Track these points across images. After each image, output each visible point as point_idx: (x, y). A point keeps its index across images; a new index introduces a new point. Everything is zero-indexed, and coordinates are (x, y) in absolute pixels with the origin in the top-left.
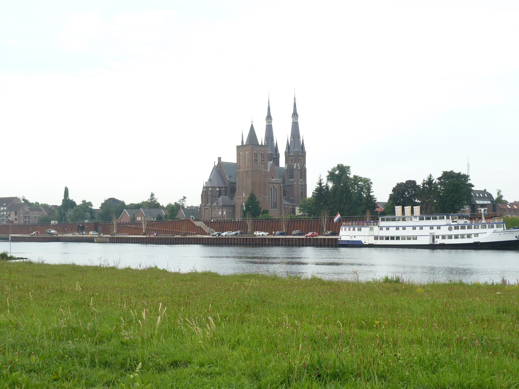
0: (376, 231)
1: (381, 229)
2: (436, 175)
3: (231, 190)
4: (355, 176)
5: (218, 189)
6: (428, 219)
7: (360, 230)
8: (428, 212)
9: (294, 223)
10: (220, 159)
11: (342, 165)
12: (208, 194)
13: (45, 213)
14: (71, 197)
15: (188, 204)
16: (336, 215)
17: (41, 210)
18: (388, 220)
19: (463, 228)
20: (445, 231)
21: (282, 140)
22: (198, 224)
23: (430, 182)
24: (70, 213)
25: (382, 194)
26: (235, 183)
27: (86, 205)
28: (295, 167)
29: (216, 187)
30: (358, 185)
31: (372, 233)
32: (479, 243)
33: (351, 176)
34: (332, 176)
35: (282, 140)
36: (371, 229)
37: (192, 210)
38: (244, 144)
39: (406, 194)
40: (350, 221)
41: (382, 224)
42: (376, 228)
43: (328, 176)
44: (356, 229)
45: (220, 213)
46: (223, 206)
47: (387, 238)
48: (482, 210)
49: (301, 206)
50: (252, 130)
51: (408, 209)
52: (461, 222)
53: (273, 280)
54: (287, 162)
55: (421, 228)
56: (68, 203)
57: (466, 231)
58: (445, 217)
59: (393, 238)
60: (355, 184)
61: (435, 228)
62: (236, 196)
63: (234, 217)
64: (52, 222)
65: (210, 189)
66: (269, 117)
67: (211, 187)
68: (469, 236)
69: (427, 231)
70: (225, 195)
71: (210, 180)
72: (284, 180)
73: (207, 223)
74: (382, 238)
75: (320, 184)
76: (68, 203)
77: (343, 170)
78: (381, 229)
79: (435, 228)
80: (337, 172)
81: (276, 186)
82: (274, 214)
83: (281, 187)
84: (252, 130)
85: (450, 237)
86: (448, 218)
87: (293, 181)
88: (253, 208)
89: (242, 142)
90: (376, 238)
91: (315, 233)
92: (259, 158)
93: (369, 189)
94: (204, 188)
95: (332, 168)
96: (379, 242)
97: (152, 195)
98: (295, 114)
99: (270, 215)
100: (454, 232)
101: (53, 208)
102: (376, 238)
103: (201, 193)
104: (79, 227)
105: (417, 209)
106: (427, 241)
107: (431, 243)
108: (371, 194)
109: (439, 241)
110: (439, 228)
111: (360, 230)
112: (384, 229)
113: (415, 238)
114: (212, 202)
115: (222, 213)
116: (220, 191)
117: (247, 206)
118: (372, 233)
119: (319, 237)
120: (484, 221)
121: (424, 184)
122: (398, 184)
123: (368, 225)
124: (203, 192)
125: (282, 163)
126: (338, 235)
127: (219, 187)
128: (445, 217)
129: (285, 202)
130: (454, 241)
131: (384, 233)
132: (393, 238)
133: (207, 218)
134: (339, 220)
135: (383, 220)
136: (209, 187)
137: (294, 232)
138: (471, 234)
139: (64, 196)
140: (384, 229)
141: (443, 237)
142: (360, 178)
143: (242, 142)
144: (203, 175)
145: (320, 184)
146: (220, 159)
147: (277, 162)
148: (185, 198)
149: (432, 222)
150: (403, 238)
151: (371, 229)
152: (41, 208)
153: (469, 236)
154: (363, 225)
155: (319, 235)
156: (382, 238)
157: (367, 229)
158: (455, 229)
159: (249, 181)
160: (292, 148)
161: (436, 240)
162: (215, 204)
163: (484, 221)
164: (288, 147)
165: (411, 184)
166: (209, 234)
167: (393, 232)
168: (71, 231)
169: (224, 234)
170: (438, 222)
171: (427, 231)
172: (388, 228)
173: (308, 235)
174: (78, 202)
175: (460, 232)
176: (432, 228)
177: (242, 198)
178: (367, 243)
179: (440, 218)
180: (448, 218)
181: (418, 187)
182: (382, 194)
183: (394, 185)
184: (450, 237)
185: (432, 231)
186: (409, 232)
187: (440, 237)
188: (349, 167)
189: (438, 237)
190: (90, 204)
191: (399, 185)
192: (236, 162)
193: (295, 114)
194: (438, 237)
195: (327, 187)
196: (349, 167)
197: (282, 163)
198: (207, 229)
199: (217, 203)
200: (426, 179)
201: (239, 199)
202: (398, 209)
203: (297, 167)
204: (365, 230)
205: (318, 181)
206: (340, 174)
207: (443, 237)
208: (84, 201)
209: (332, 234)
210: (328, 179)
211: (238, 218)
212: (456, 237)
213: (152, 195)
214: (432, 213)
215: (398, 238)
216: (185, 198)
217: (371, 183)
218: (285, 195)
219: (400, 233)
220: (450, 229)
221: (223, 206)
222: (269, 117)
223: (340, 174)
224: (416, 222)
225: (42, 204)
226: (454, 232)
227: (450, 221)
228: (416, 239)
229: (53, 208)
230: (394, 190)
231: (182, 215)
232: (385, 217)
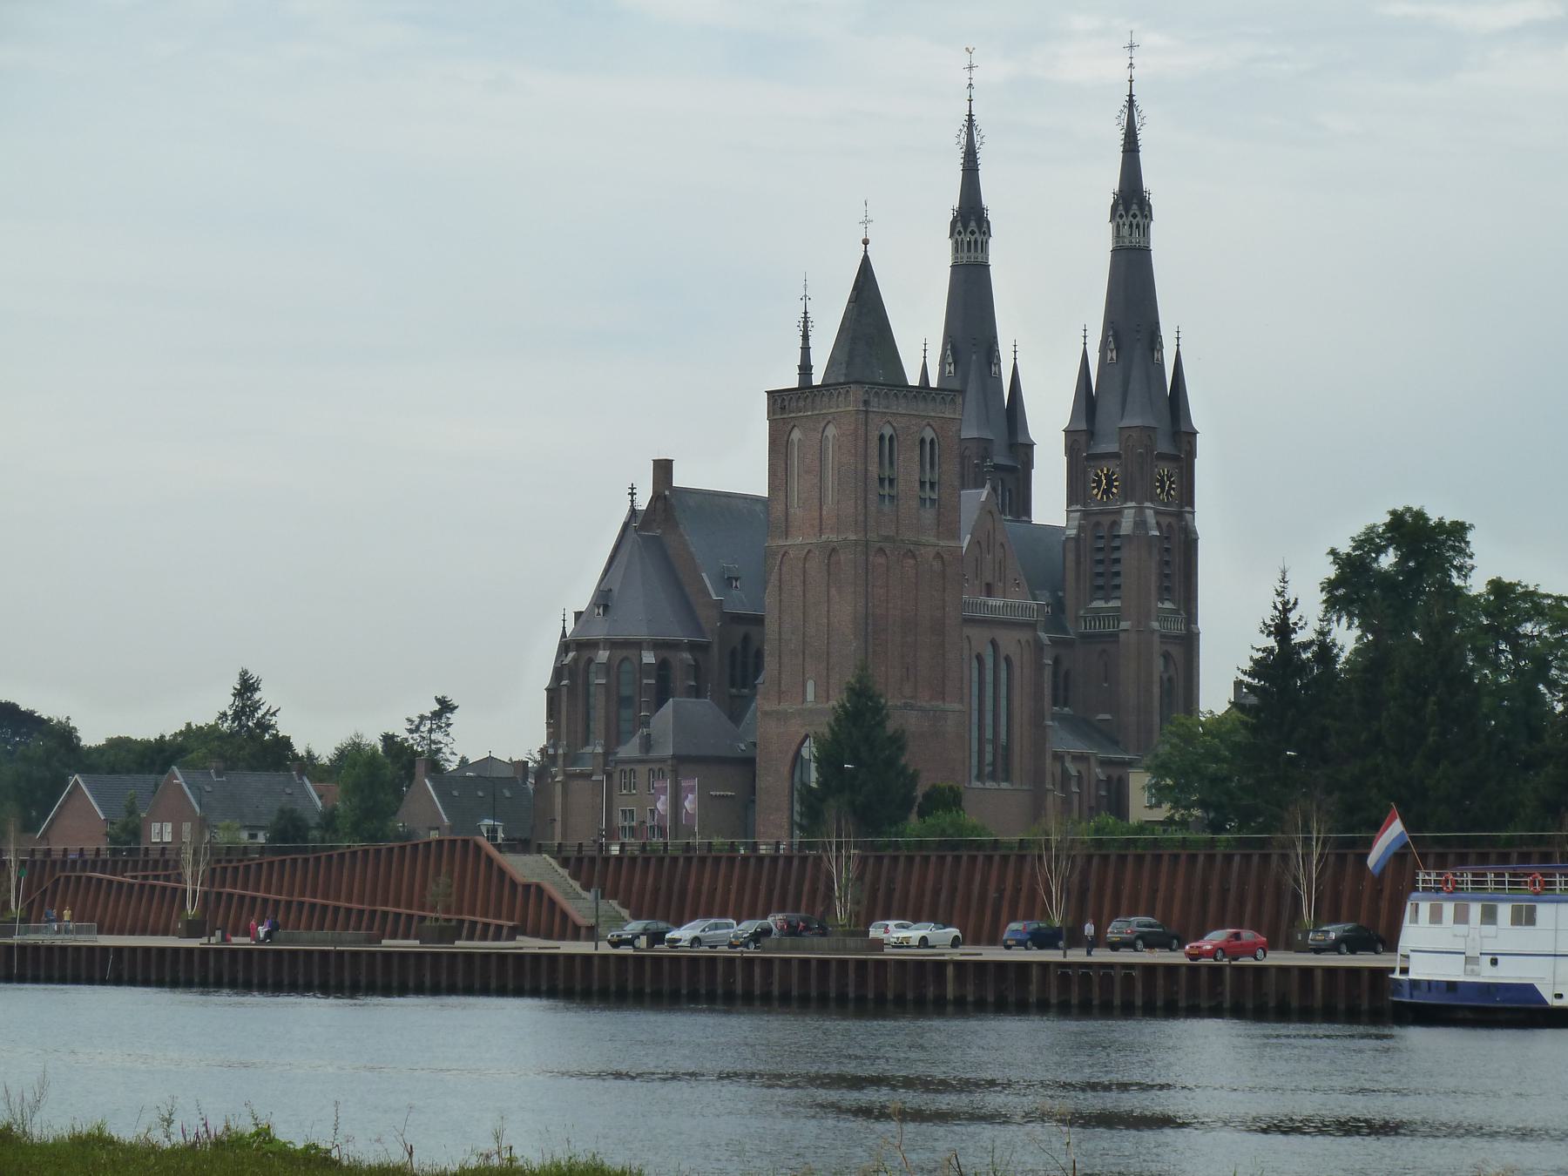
3: (730, 660)
4: (1498, 587)
5: (649, 658)
7: (1525, 917)
9: (1113, 873)
10: (663, 469)
11: (1420, 516)
12: (585, 681)
15: (465, 744)
16: (1377, 826)
21: (1048, 355)
22: (525, 867)
26: (759, 621)
28: (1126, 526)
29: (638, 645)
30: (1514, 639)
33: (1477, 585)
34: (1352, 584)
35: (1048, 355)
37: (488, 783)
38: (817, 379)
40: (1462, 860)
43: (1330, 586)
44: (1504, 911)
45: (663, 805)
49: (1161, 769)
50: (865, 291)
54: (1076, 491)
60: (1495, 632)
62: (763, 703)
63: (745, 826)
65: (603, 655)
66: (970, 220)
67: (613, 645)
70: (697, 692)
71: (604, 599)
72: (1058, 606)
73: (582, 865)
75: (1282, 630)
80: (1387, 560)
81: (1010, 642)
82: (995, 812)
83: (1038, 647)
84: (865, 291)
87: (1117, 614)
88: (865, 772)
89: (805, 368)
91: (1247, 935)
92: (908, 469)
94: (565, 646)
95: (1358, 529)
97: (247, 687)
98: (1131, 203)
99: (970, 817)
103: (546, 678)
111: (1525, 917)
114: (615, 738)
115: (672, 807)
116: (663, 666)
117: (828, 761)
119: (1275, 959)
124: (558, 673)
125: (1050, 501)
126: (1391, 944)
127: (656, 646)
129: (1064, 742)
133: (583, 835)
134: (1399, 857)
136: (592, 645)
137: (1115, 930)
142: (1530, 595)
143: (805, 368)
145: (1282, 630)
146: (663, 469)
148: (445, 707)
154: (1545, 890)
155: (1272, 945)
159: (845, 610)
160: (1108, 408)
164: (1087, 402)
166: (592, 933)
169: (684, 933)
173: (1207, 944)
177: (794, 716)
188: (1459, 530)
192: (761, 489)
193: (1131, 203)
195: (1325, 651)
196: (1459, 530)
197: (1050, 501)
198: (580, 904)
199: (647, 744)
203: (1140, 523)
205: (1269, 614)
209: (1353, 944)
210: (1332, 604)
211: (775, 833)
213: (247, 687)
216: (445, 707)
218: (1062, 691)
222: (970, 220)
231: (425, 813)
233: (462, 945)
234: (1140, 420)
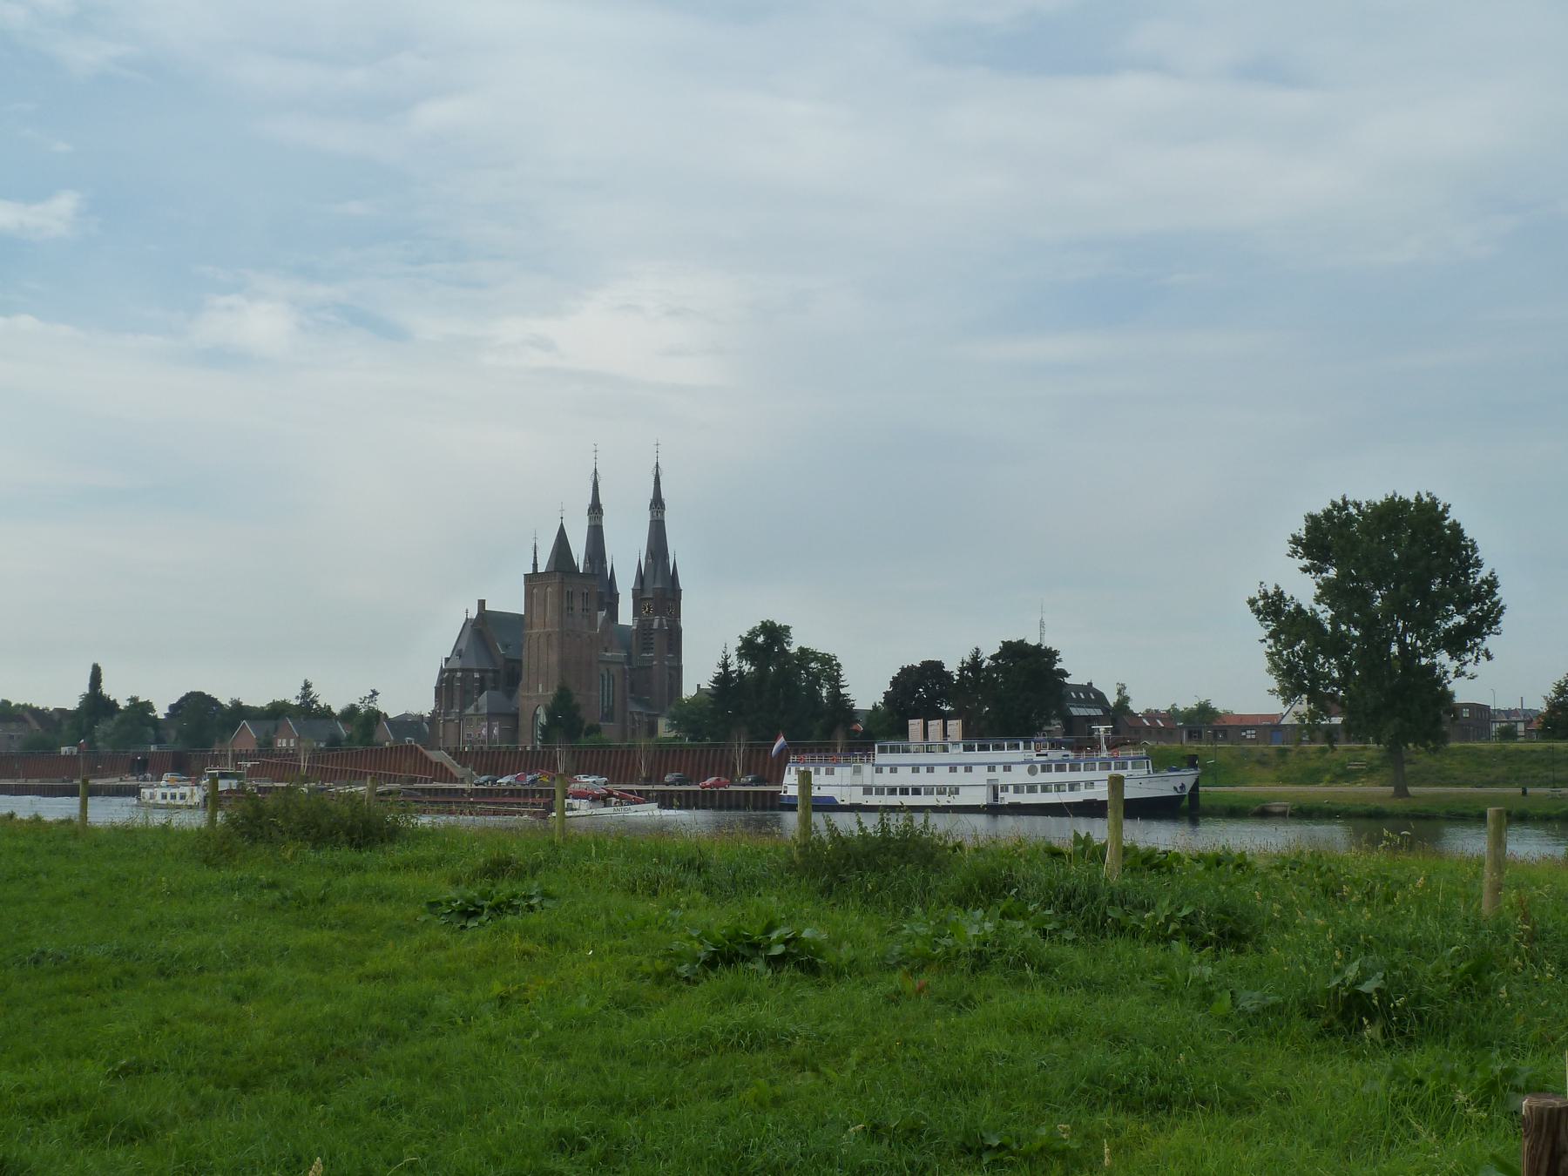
0: (868, 774)
1: (879, 770)
2: (990, 648)
3: (509, 677)
4: (801, 650)
5: (477, 675)
6: (983, 748)
7: (830, 772)
8: (982, 733)
9: (665, 758)
10: (482, 603)
11: (772, 623)
12: (450, 686)
13: (35, 726)
14: (109, 689)
15: (391, 707)
16: (776, 739)
17: (25, 721)
18: (893, 750)
19: (1060, 768)
20: (1020, 775)
21: (625, 559)
22: (436, 756)
23: (974, 665)
24: (104, 727)
25: (866, 689)
26: (520, 662)
27: (141, 709)
28: (655, 625)
29: (472, 671)
30: (807, 669)
31: (858, 780)
32: (1094, 801)
33: (793, 649)
34: (748, 648)
35: (625, 559)
36: (857, 771)
37: (407, 724)
38: (541, 569)
39: (920, 692)
40: (804, 752)
41: (881, 759)
42: (867, 769)
43: (739, 649)
44: (823, 770)
45: (484, 732)
46: (491, 716)
47: (892, 791)
48: (1102, 728)
49: (673, 717)
50: (562, 538)
51: (935, 726)
52: (1056, 755)
53: (1239, 866)
54: (636, 612)
55: (968, 769)
56: (96, 703)
57: (1068, 776)
58: (1021, 744)
59: (904, 791)
60: (801, 667)
61: (999, 768)
62: (522, 692)
63: (514, 740)
64: (64, 750)
65: (459, 674)
66: (596, 509)
67: (462, 670)
68: (1073, 786)
69: (981, 775)
70: (495, 688)
71: (457, 652)
72: (629, 657)
73: (458, 755)
74: (880, 791)
75: (725, 666)
76: (96, 703)
77: (774, 633)
78: (879, 770)
79: (999, 768)
80: (760, 640)
81: (614, 669)
82: (610, 733)
83: (624, 671)
84: (562, 538)
85: (1032, 789)
86: (1027, 747)
87: (652, 659)
88: (566, 719)
89: (535, 565)
90: (867, 790)
91: (723, 780)
92: (578, 604)
93: (835, 680)
94: (442, 671)
95: (750, 628)
96: (874, 800)
97: (307, 686)
98: (657, 504)
99: (604, 736)
100: (1042, 778)
101: (57, 717)
102: (867, 790)
103: (434, 682)
104: (134, 760)
105: (955, 726)
106: (981, 797)
107: (991, 801)
108: (843, 691)
109: (1008, 798)
110: (1007, 768)
111: (830, 772)
112: (886, 770)
113: (955, 791)
114: (464, 707)
115: (483, 732)
116: (482, 679)
117: (551, 714)
118: (858, 780)
119: (732, 788)
120: (1105, 754)
121: (962, 670)
122: (903, 669)
123: (847, 763)
124: (441, 681)
125: (626, 616)
126: (779, 781)
127: (479, 671)
128: (1021, 744)
129: (635, 708)
130: (1067, 797)
131: (887, 779)
132: (904, 791)
133: (452, 745)
134: (781, 751)
135: (883, 750)
136: (455, 670)
137: (668, 778)
138: (1078, 783)
139: (91, 685)
140: (886, 770)
141: (1017, 789)
142: (814, 653)
143: (535, 565)
144: (439, 642)
145: (725, 666)
146: (482, 603)
147: (613, 615)
148: (375, 693)
149: (991, 756)
150: (929, 792)
151: (857, 771)
152: (27, 715)
153: (1073, 786)
154: (837, 763)
155: (732, 783)
156: (880, 791)
157: (848, 771)
158: (1043, 770)
159: (554, 658)
160: (648, 582)
161: (1001, 795)
162: (470, 710)
163: (1105, 754)
164: (641, 578)
165: (933, 669)
166: (462, 781)
167: (905, 777)
168: (113, 770)
169: (504, 781)
170: (1007, 755)
171: (981, 775)
172: (894, 770)
173: (708, 782)
174: (123, 704)
175: (1054, 777)
176: (991, 768)
177: (536, 700)
178: (847, 803)
179: (1010, 748)
180: (1027, 747)
181: (949, 675)
182: (866, 689)
183: (896, 672)
184: (1032, 789)
185: (992, 775)
186: (942, 777)
187: (1011, 788)
188: (787, 628)
189: (1005, 788)
190: (148, 706)
191: (906, 672)
192: (519, 609)
193: (657, 504)
194: (1005, 788)
195: (741, 673)
196: (787, 628)
197: (626, 616)
198: (457, 770)
199: (477, 709)
200: (968, 659)
201: (529, 698)
202: (915, 725)
203: (661, 624)
204: (843, 773)
205: (720, 660)
206: (767, 643)
207: (1017, 789)
208: (134, 700)
209: (757, 782)
210: (740, 656)
211: (529, 741)
212: (1045, 788)
213: (307, 686)
214: (980, 736)
215: (916, 791)
216: (375, 693)
217: (839, 665)
218: (632, 691)
219: (922, 779)
220: (1032, 771)
221: (491, 716)
222: (596, 509)
223: (767, 643)
224: (957, 754)
225: (18, 706)
226: (1042, 778)
227: (1032, 755)
228: (957, 792)
229: (57, 717)
230: (895, 682)
231: (385, 737)
232: (889, 744)
233: (416, 785)
234: (661, 590)
